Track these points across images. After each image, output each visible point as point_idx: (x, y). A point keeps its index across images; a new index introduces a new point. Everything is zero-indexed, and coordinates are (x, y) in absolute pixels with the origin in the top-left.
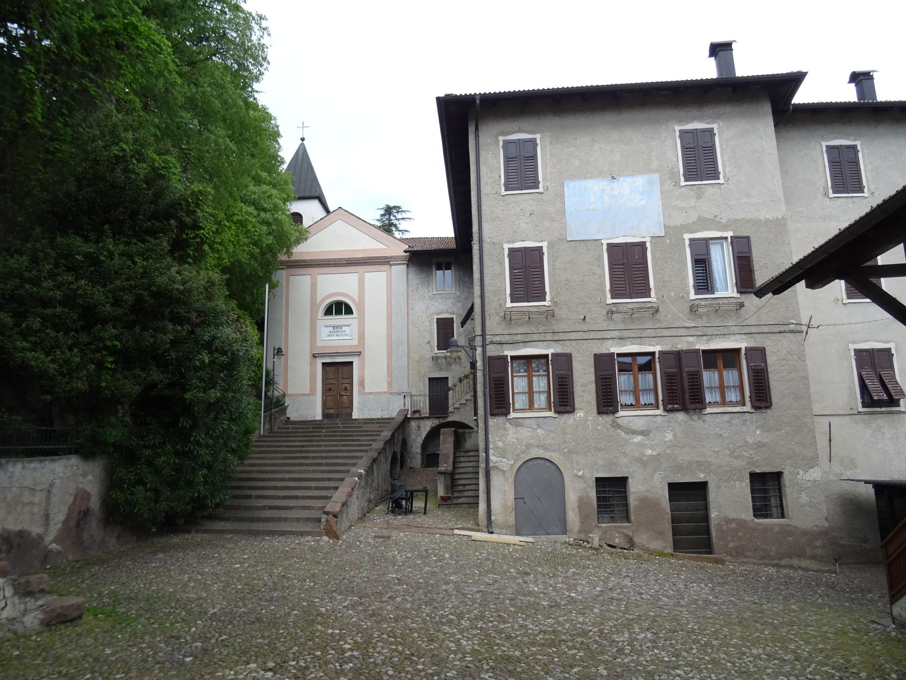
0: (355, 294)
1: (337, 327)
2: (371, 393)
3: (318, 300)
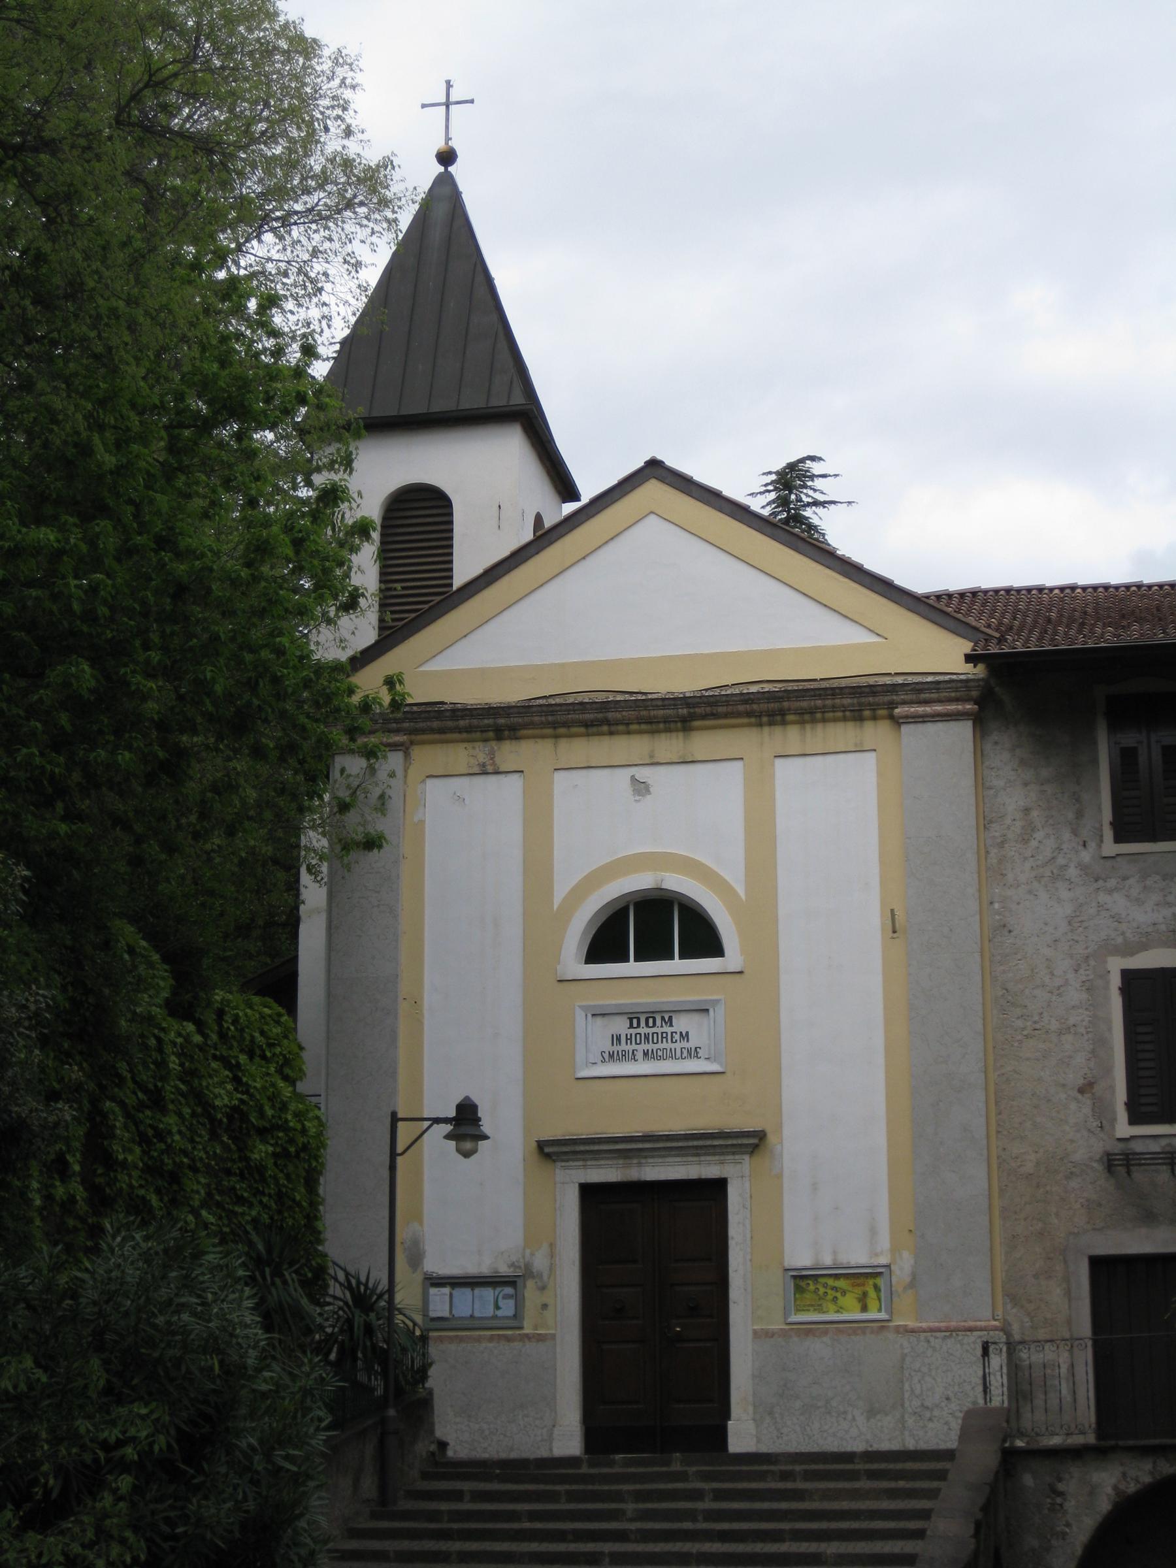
1: (651, 1016)
3: (560, 892)
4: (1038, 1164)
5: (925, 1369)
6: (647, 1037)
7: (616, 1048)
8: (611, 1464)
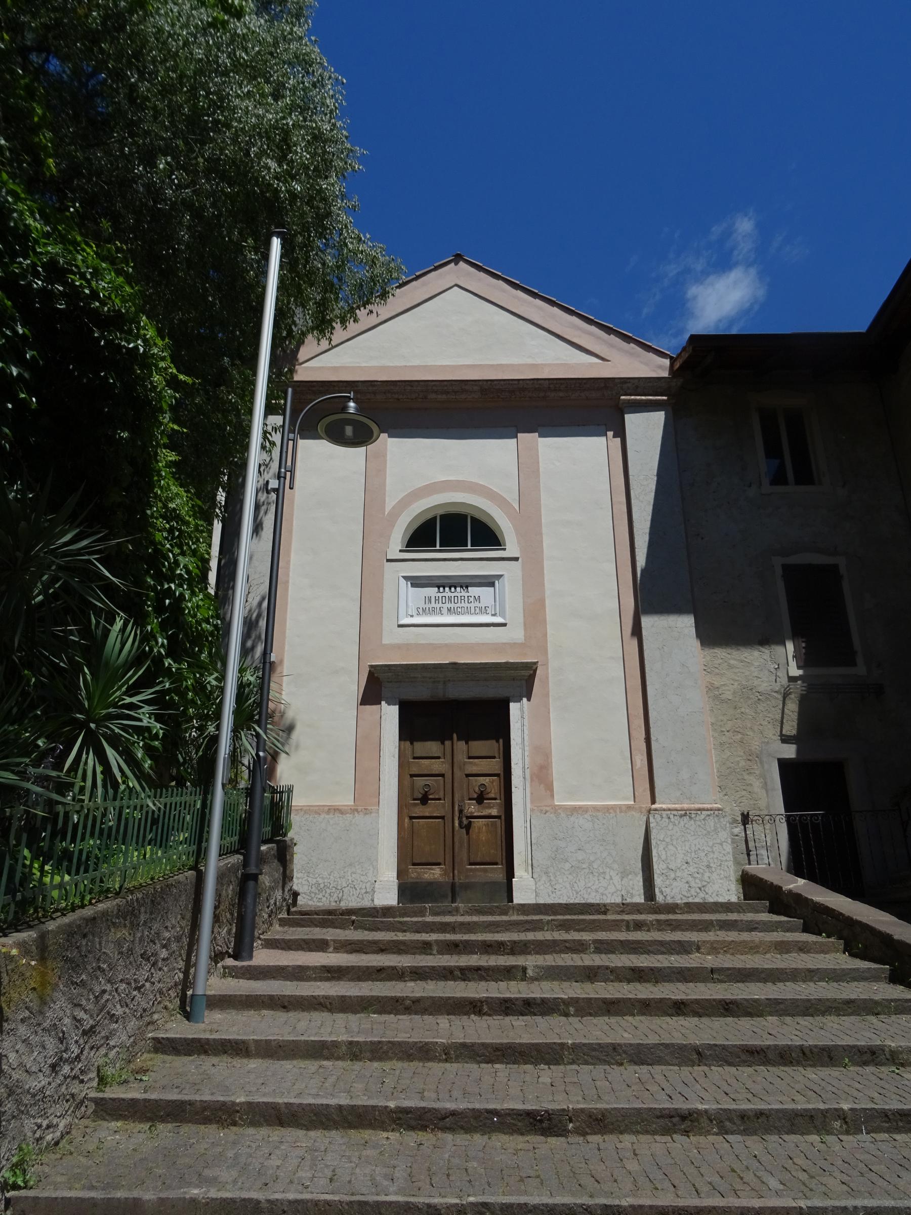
0: (508, 488)
2: (575, 810)
3: (390, 503)
4: (734, 693)
5: (668, 840)
6: (450, 598)
7: (427, 606)
8: (422, 913)
